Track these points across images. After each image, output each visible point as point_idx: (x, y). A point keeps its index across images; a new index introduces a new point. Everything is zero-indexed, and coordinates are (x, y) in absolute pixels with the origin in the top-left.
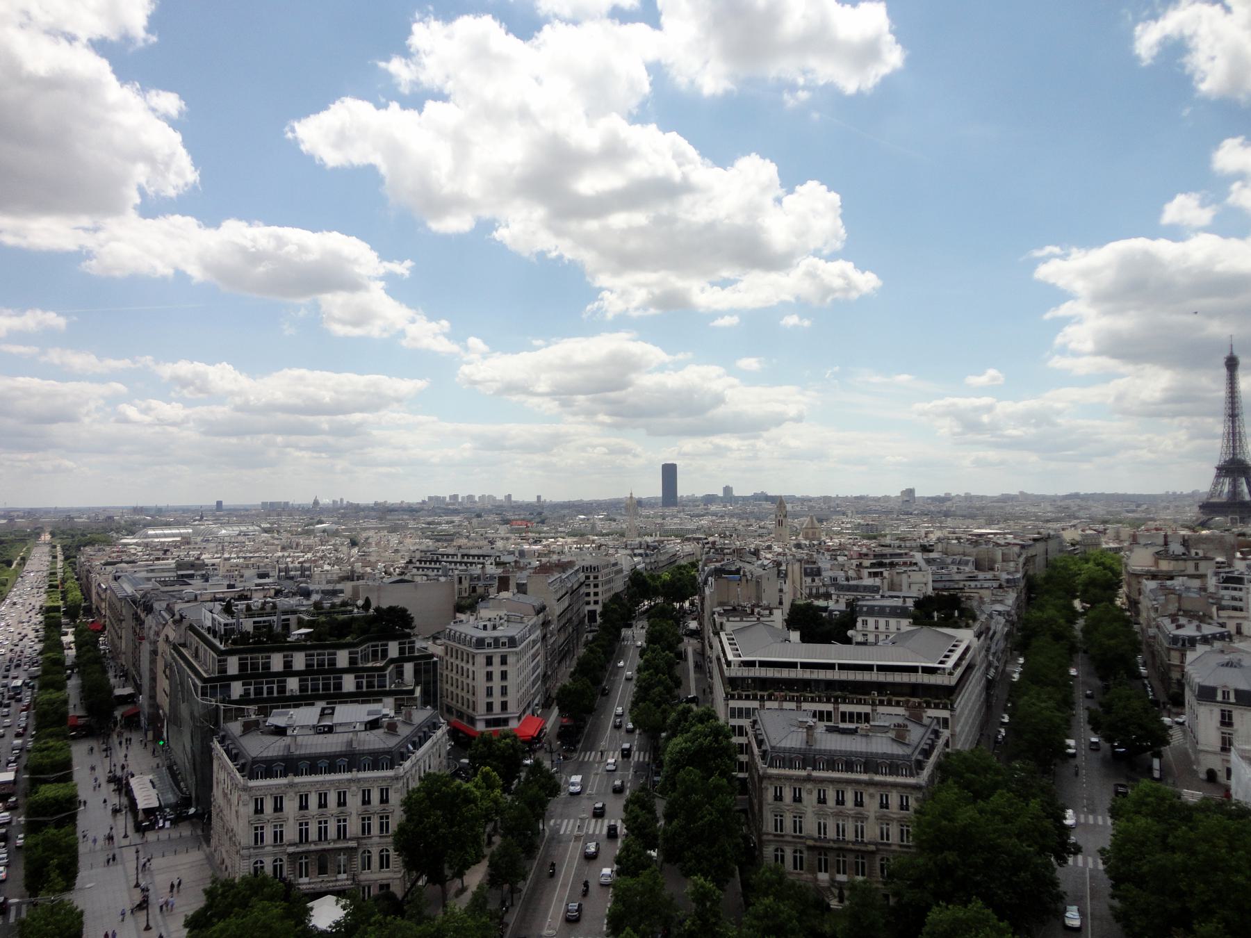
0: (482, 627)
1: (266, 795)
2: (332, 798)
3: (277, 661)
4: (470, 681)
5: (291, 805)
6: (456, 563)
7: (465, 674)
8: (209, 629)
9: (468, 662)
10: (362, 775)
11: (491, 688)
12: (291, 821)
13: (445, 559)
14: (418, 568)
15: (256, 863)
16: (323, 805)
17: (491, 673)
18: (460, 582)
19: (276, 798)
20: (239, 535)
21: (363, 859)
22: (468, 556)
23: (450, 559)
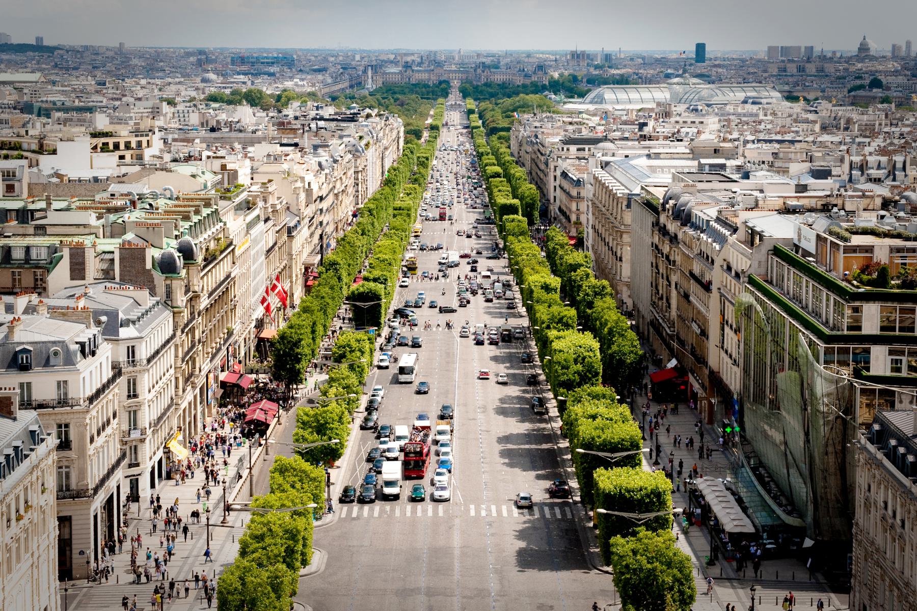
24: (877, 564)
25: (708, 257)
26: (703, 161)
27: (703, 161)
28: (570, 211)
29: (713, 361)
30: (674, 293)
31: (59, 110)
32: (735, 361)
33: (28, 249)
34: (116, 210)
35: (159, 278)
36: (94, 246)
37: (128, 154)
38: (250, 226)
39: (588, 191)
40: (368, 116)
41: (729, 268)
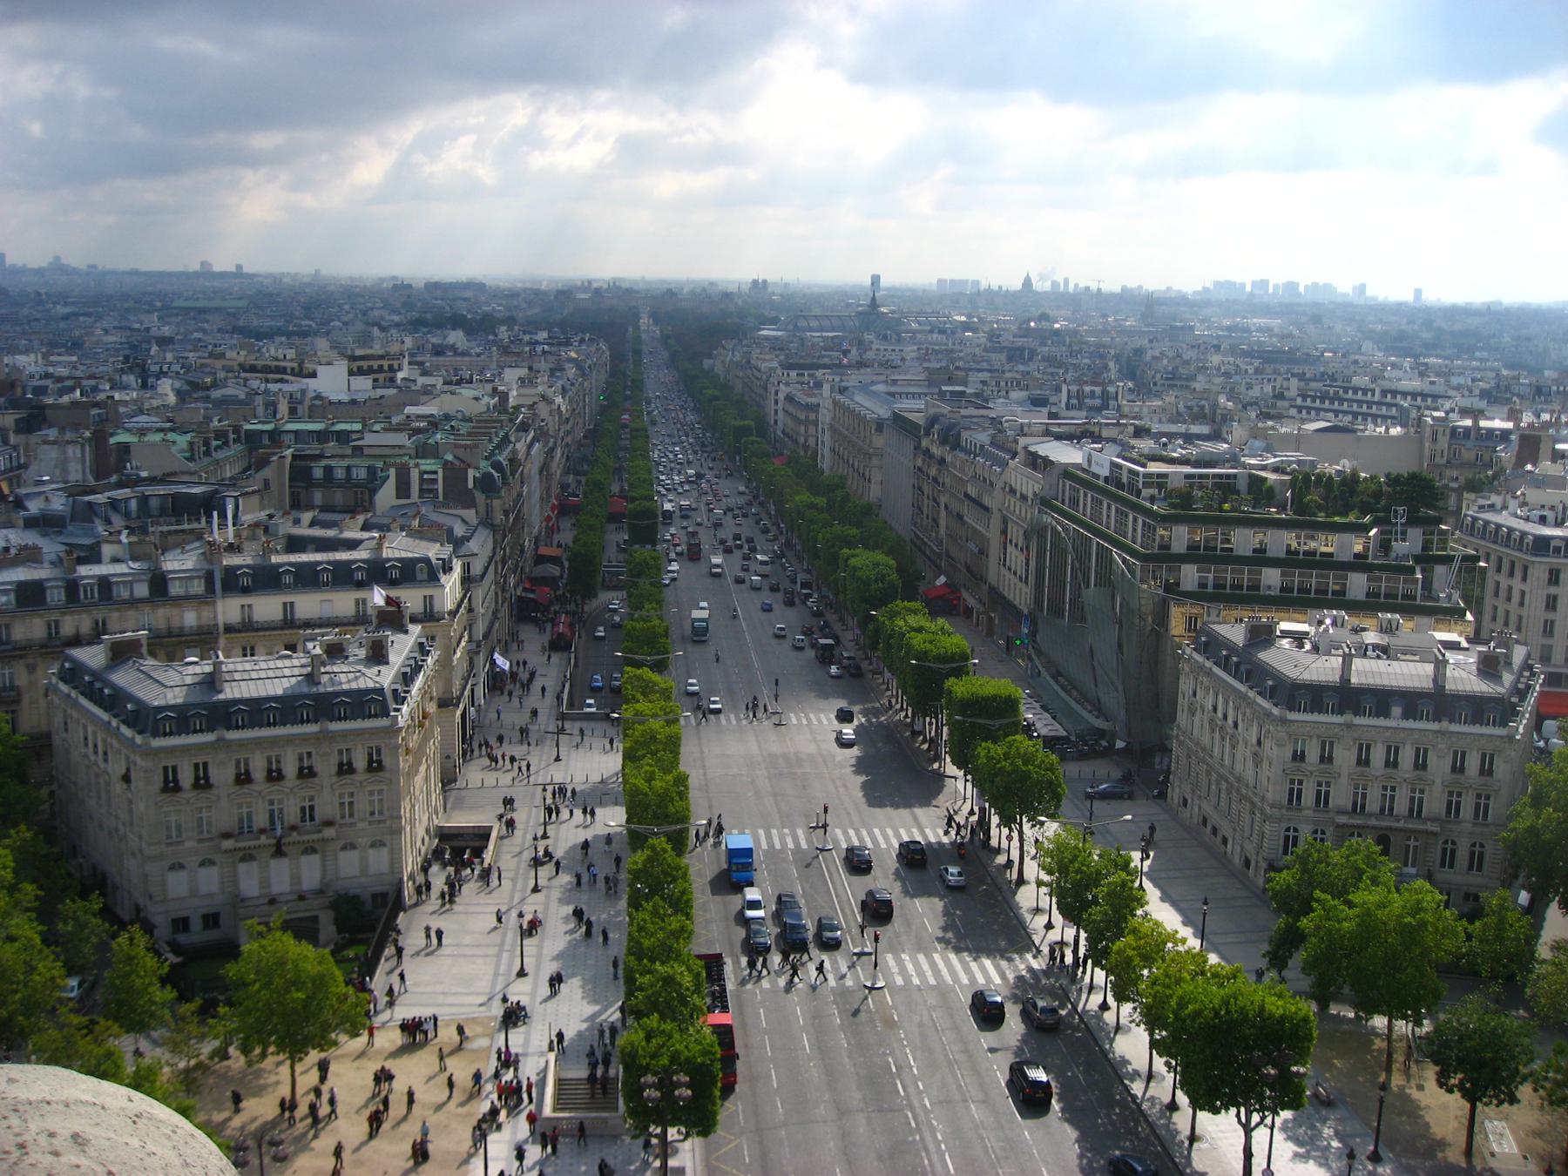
0: (1537, 519)
1: (1311, 737)
2: (1407, 756)
3: (1244, 540)
4: (1513, 607)
5: (1345, 757)
6: (1370, 404)
7: (1503, 594)
8: (1106, 479)
9: (1511, 574)
10: (1455, 728)
11: (1552, 622)
12: (1344, 780)
13: (1350, 395)
14: (1300, 409)
15: (1288, 830)
16: (1392, 763)
17: (1555, 598)
18: (1435, 440)
19: (1324, 743)
20: (931, 331)
21: (1445, 850)
22: (1394, 393)
23: (1360, 396)
24: (1204, 761)
25: (985, 480)
26: (944, 388)
27: (944, 388)
28: (798, 434)
29: (992, 578)
30: (943, 513)
31: (281, 335)
32: (1021, 578)
33: (348, 469)
34: (418, 431)
35: (480, 497)
36: (417, 465)
37: (381, 376)
38: (530, 446)
39: (825, 416)
40: (582, 341)
41: (1013, 491)
